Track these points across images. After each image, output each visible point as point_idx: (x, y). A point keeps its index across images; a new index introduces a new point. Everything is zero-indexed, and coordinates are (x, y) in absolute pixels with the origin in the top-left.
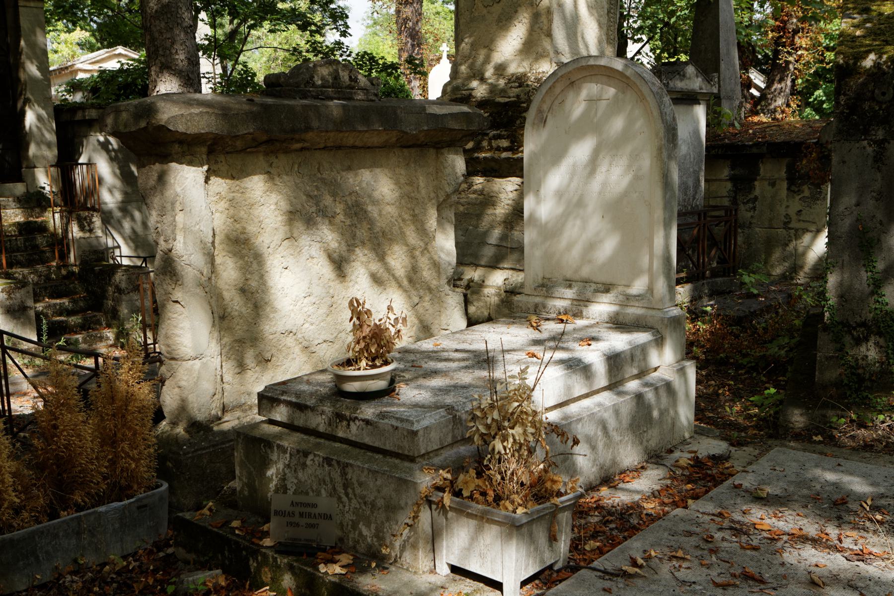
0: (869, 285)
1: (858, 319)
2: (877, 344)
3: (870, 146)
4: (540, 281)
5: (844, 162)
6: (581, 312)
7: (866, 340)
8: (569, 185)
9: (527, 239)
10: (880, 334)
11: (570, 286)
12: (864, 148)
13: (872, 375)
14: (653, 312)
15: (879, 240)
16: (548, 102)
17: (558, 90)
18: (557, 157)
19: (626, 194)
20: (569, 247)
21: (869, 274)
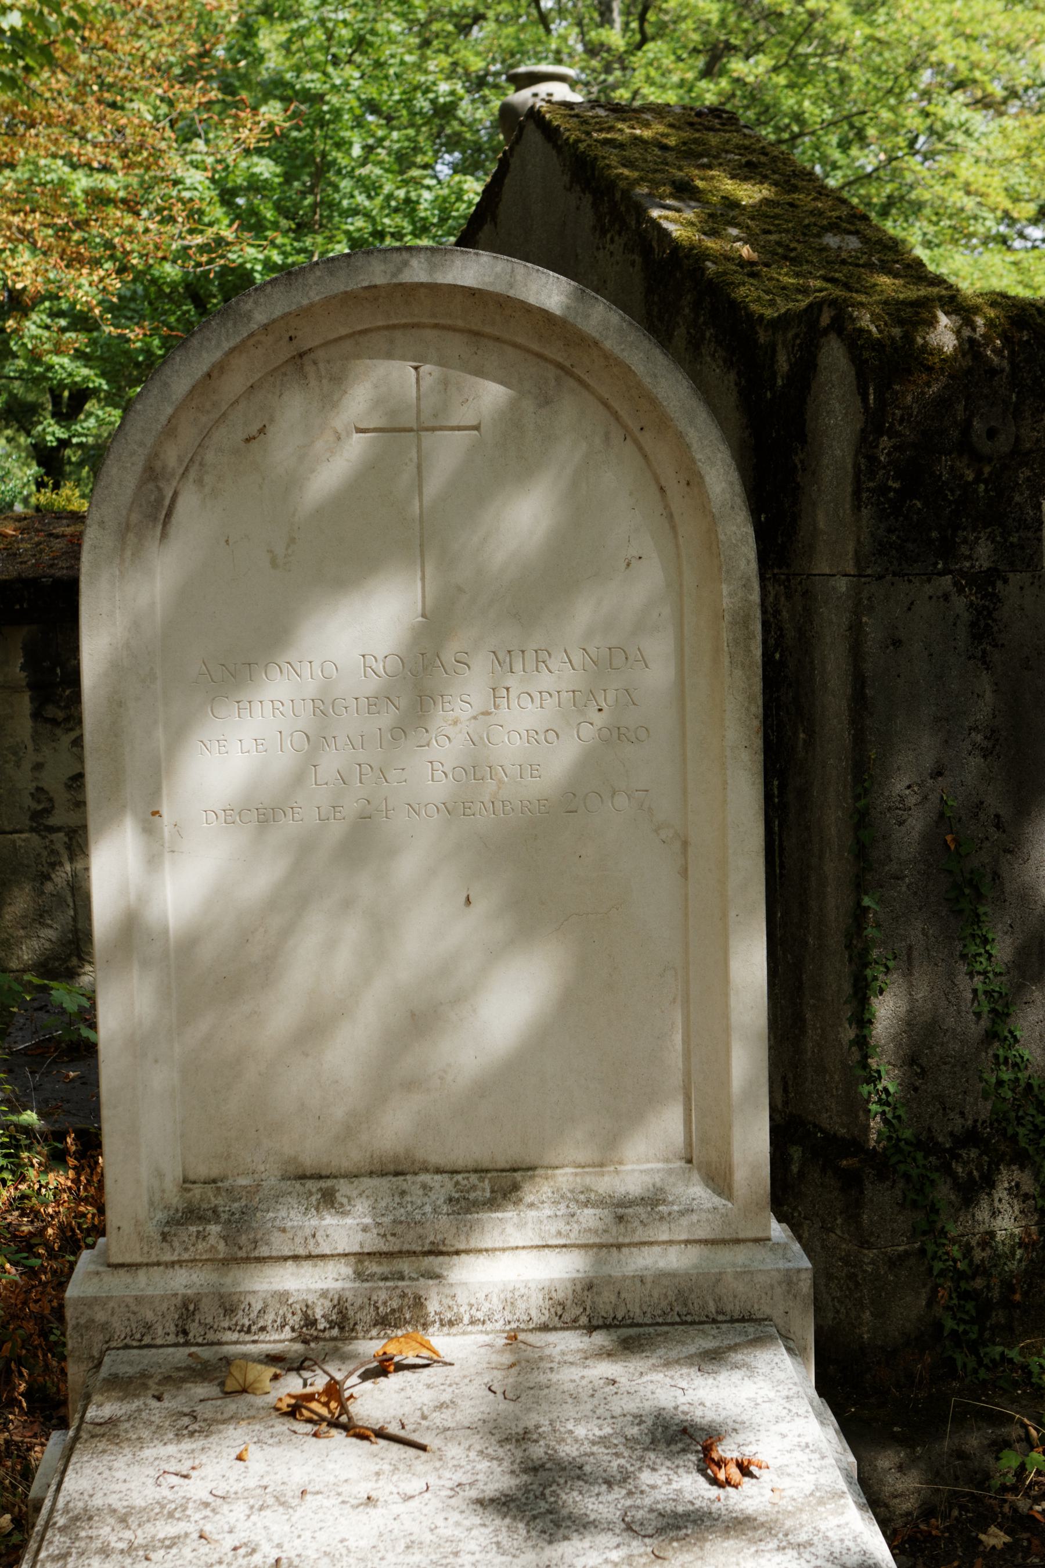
0: (978, 1015)
1: (957, 1124)
2: (1015, 1191)
3: (961, 591)
4: (174, 1199)
5: (897, 643)
6: (418, 1303)
7: (989, 1183)
8: (298, 779)
9: (112, 1023)
10: (1021, 1159)
11: (329, 1200)
12: (946, 597)
13: (1012, 1289)
14: (739, 1257)
15: (996, 876)
16: (188, 435)
17: (234, 383)
18: (231, 656)
19: (572, 801)
20: (313, 1031)
21: (978, 980)
